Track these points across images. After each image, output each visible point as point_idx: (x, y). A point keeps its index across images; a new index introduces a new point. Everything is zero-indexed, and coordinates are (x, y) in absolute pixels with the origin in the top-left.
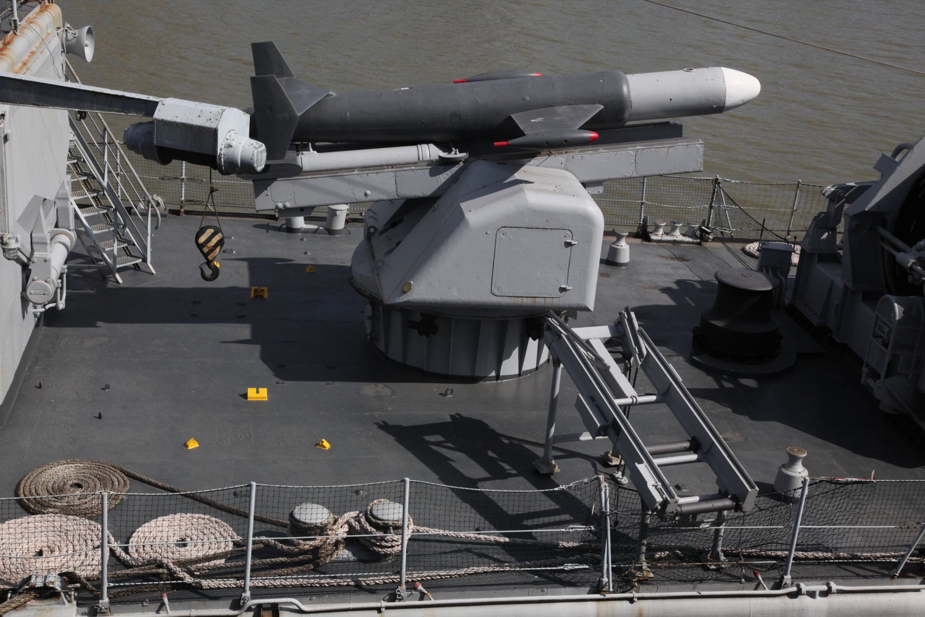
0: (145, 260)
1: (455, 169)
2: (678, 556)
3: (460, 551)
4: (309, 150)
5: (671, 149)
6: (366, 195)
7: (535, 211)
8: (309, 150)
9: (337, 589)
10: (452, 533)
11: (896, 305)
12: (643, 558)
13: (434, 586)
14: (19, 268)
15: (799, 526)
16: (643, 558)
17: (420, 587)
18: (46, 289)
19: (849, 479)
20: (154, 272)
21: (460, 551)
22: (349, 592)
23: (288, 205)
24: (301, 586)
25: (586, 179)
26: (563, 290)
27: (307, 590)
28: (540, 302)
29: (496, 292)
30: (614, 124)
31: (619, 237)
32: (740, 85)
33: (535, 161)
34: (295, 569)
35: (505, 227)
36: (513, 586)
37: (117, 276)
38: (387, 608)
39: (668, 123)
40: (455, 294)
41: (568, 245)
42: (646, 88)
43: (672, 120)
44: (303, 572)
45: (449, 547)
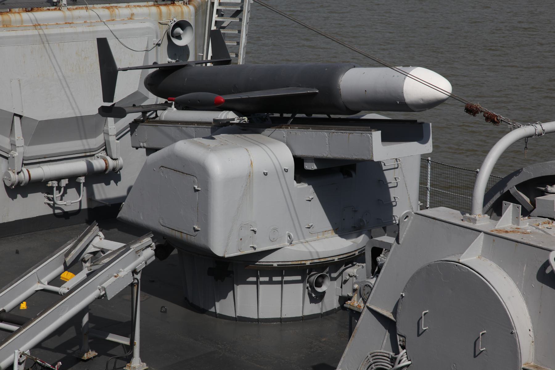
5: (351, 135)
7: (177, 156)
18: (10, 177)
25: (299, 153)
33: (268, 131)
39: (415, 122)
41: (196, 191)
42: (357, 80)
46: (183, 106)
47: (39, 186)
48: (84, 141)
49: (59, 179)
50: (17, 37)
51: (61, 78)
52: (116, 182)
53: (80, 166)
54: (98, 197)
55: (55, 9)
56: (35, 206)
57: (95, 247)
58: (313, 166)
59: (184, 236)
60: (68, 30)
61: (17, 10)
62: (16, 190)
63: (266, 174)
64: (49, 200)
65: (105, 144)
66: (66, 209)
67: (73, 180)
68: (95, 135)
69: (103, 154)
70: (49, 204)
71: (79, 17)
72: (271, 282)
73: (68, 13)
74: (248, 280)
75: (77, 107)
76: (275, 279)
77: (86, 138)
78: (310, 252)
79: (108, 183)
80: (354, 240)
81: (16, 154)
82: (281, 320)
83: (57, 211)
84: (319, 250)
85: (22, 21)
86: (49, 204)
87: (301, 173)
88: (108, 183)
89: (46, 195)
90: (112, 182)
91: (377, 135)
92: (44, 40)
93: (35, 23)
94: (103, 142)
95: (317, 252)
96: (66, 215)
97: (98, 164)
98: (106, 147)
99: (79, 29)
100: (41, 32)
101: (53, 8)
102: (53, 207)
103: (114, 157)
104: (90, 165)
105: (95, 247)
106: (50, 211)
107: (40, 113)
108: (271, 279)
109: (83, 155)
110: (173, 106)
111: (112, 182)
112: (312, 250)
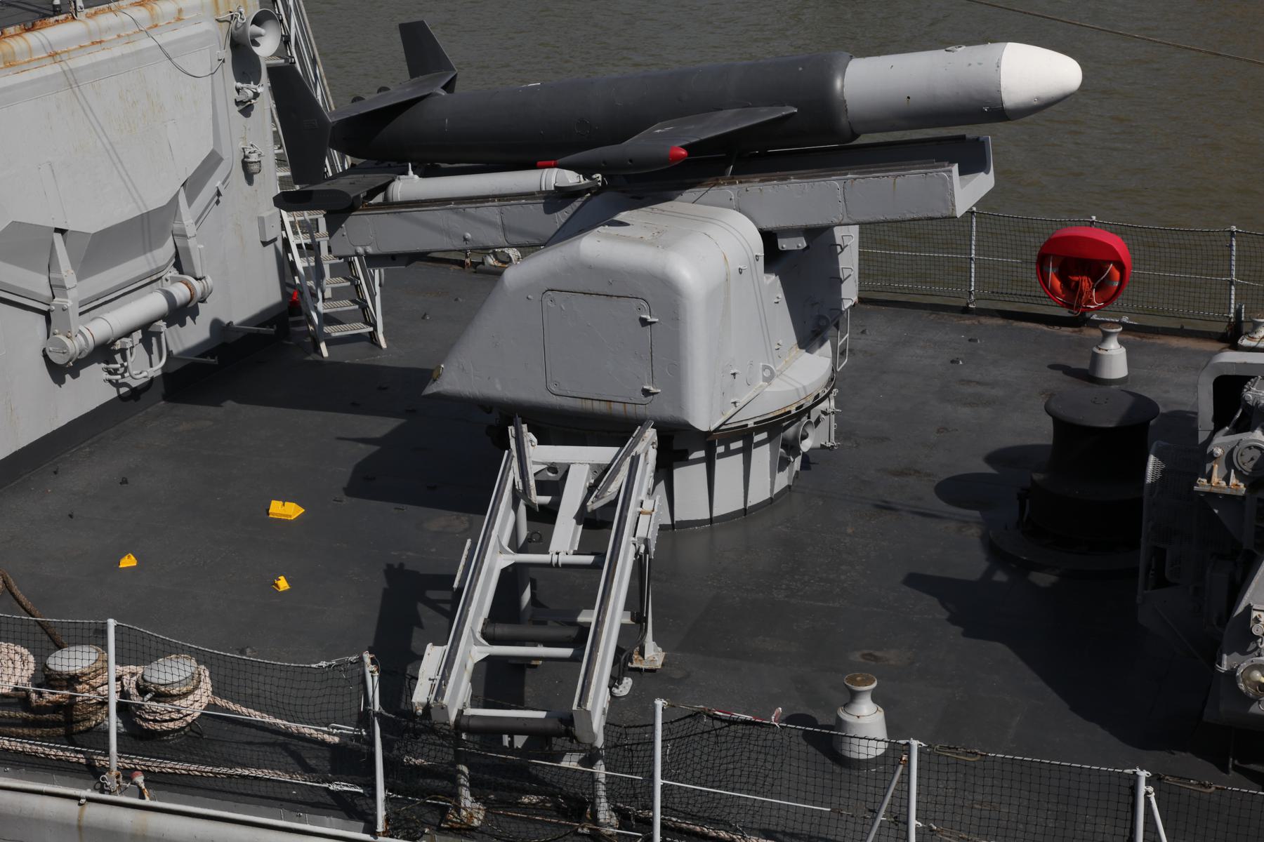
0: (376, 329)
1: (577, 204)
2: (558, 808)
3: (273, 744)
4: (406, 173)
6: (465, 239)
7: (590, 267)
8: (406, 173)
9: (57, 763)
10: (272, 720)
11: (1152, 458)
12: (465, 792)
13: (157, 781)
14: (42, 319)
15: (659, 782)
16: (465, 792)
17: (140, 779)
19: (736, 715)
20: (384, 345)
21: (273, 744)
22: (79, 771)
23: (370, 250)
24: (16, 752)
26: (646, 393)
27: (30, 760)
28: (618, 408)
29: (553, 389)
30: (796, 135)
31: (1106, 336)
32: (1034, 71)
34: (39, 732)
35: (552, 289)
36: (248, 798)
37: (323, 346)
38: (89, 800)
40: (498, 386)
41: (644, 322)
43: (970, 132)
44: (29, 737)
45: (269, 737)
46: (427, 171)
47: (104, 352)
48: (149, 255)
49: (128, 334)
50: (32, 82)
51: (109, 147)
52: (194, 319)
53: (151, 304)
54: (176, 350)
55: (66, 20)
56: (93, 389)
57: (534, 463)
58: (801, 243)
59: (630, 408)
60: (101, 55)
61: (11, 30)
62: (58, 372)
63: (740, 271)
64: (110, 373)
65: (177, 255)
66: (134, 384)
67: (147, 331)
68: (160, 243)
69: (174, 273)
70: (110, 381)
71: (109, 29)
72: (729, 453)
73: (91, 23)
74: (691, 457)
75: (140, 196)
76: (734, 446)
77: (151, 250)
78: (797, 389)
79: (183, 324)
80: (818, 352)
81: (69, 303)
82: (745, 511)
83: (123, 390)
84: (806, 383)
85: (30, 50)
86: (110, 381)
87: (773, 256)
88: (183, 324)
89: (103, 365)
90: (188, 319)
91: (955, 168)
92: (71, 80)
93: (49, 51)
94: (173, 251)
95: (804, 387)
96: (136, 393)
97: (181, 293)
98: (179, 263)
99: (117, 51)
100: (66, 68)
101: (62, 17)
102: (117, 385)
103: (199, 275)
104: (169, 296)
105: (534, 463)
106: (111, 393)
107: (91, 219)
108: (727, 448)
109: (148, 280)
110: (411, 172)
111: (188, 319)
112: (798, 386)
